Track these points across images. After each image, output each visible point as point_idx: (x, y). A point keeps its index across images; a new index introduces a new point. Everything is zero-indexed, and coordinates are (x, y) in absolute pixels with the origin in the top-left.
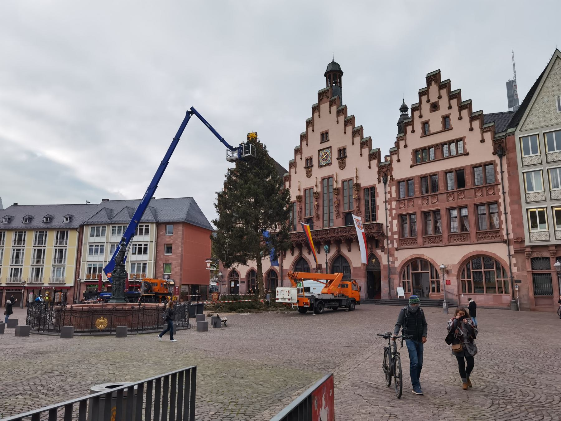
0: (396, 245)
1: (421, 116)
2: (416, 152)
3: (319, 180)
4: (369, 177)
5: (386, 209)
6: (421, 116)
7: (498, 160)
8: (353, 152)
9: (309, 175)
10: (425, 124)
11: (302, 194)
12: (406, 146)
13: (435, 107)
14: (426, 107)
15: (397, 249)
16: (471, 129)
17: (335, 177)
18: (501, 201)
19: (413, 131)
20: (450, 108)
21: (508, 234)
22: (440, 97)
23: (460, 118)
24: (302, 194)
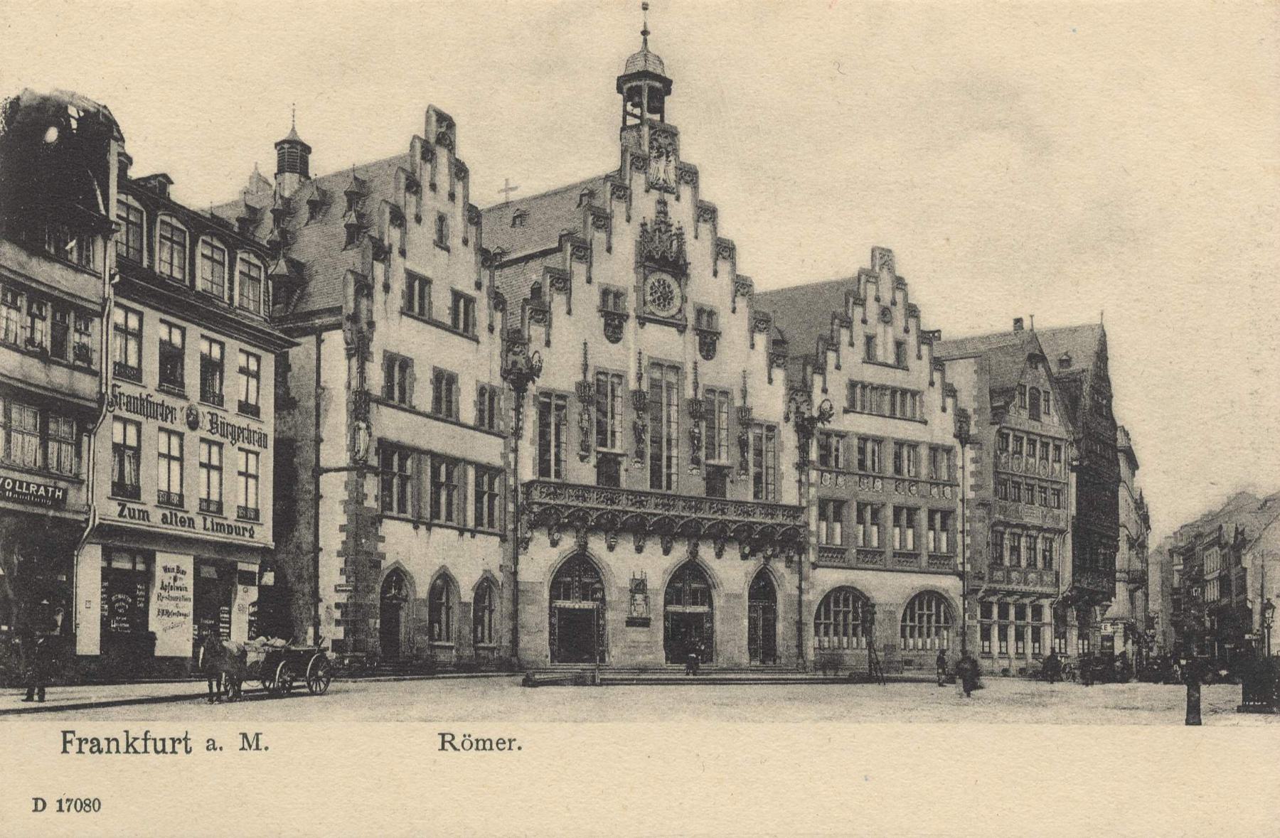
0: (812, 558)
1: (864, 321)
2: (852, 385)
3: (645, 363)
4: (770, 401)
5: (800, 481)
6: (864, 321)
7: (958, 448)
8: (734, 327)
9: (614, 331)
10: (870, 340)
11: (590, 379)
12: (838, 367)
13: (885, 315)
14: (873, 309)
15: (815, 566)
16: (932, 384)
17: (689, 367)
18: (959, 511)
19: (852, 344)
20: (907, 331)
21: (963, 564)
22: (894, 303)
23: (919, 357)
24: (590, 379)
